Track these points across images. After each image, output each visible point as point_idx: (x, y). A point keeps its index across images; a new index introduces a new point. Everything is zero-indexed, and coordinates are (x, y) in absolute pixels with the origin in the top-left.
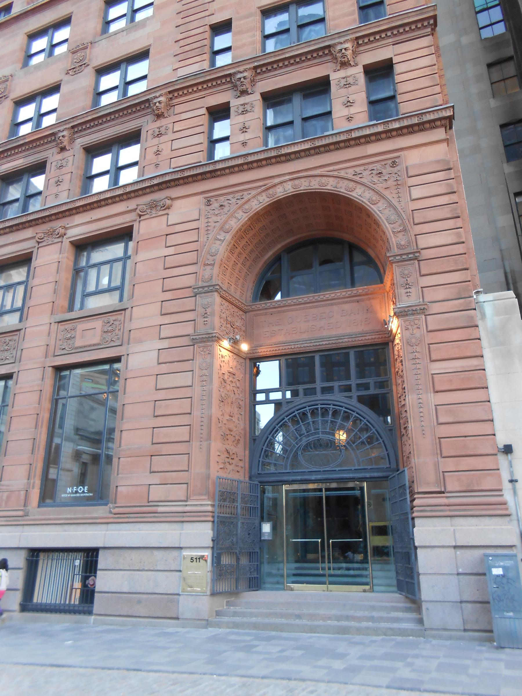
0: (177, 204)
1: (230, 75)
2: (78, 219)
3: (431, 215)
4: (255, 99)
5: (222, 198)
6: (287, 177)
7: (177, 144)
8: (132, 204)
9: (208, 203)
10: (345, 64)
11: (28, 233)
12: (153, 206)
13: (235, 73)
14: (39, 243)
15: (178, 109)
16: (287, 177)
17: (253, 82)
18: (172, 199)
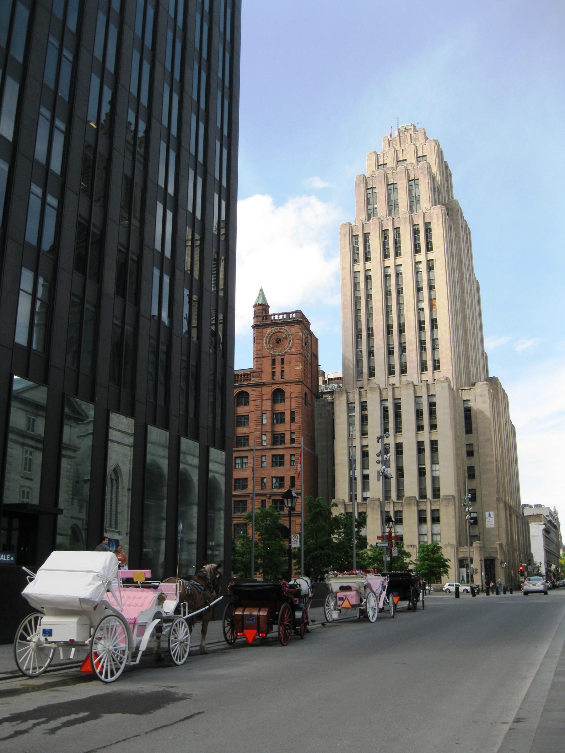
4: (271, 500)
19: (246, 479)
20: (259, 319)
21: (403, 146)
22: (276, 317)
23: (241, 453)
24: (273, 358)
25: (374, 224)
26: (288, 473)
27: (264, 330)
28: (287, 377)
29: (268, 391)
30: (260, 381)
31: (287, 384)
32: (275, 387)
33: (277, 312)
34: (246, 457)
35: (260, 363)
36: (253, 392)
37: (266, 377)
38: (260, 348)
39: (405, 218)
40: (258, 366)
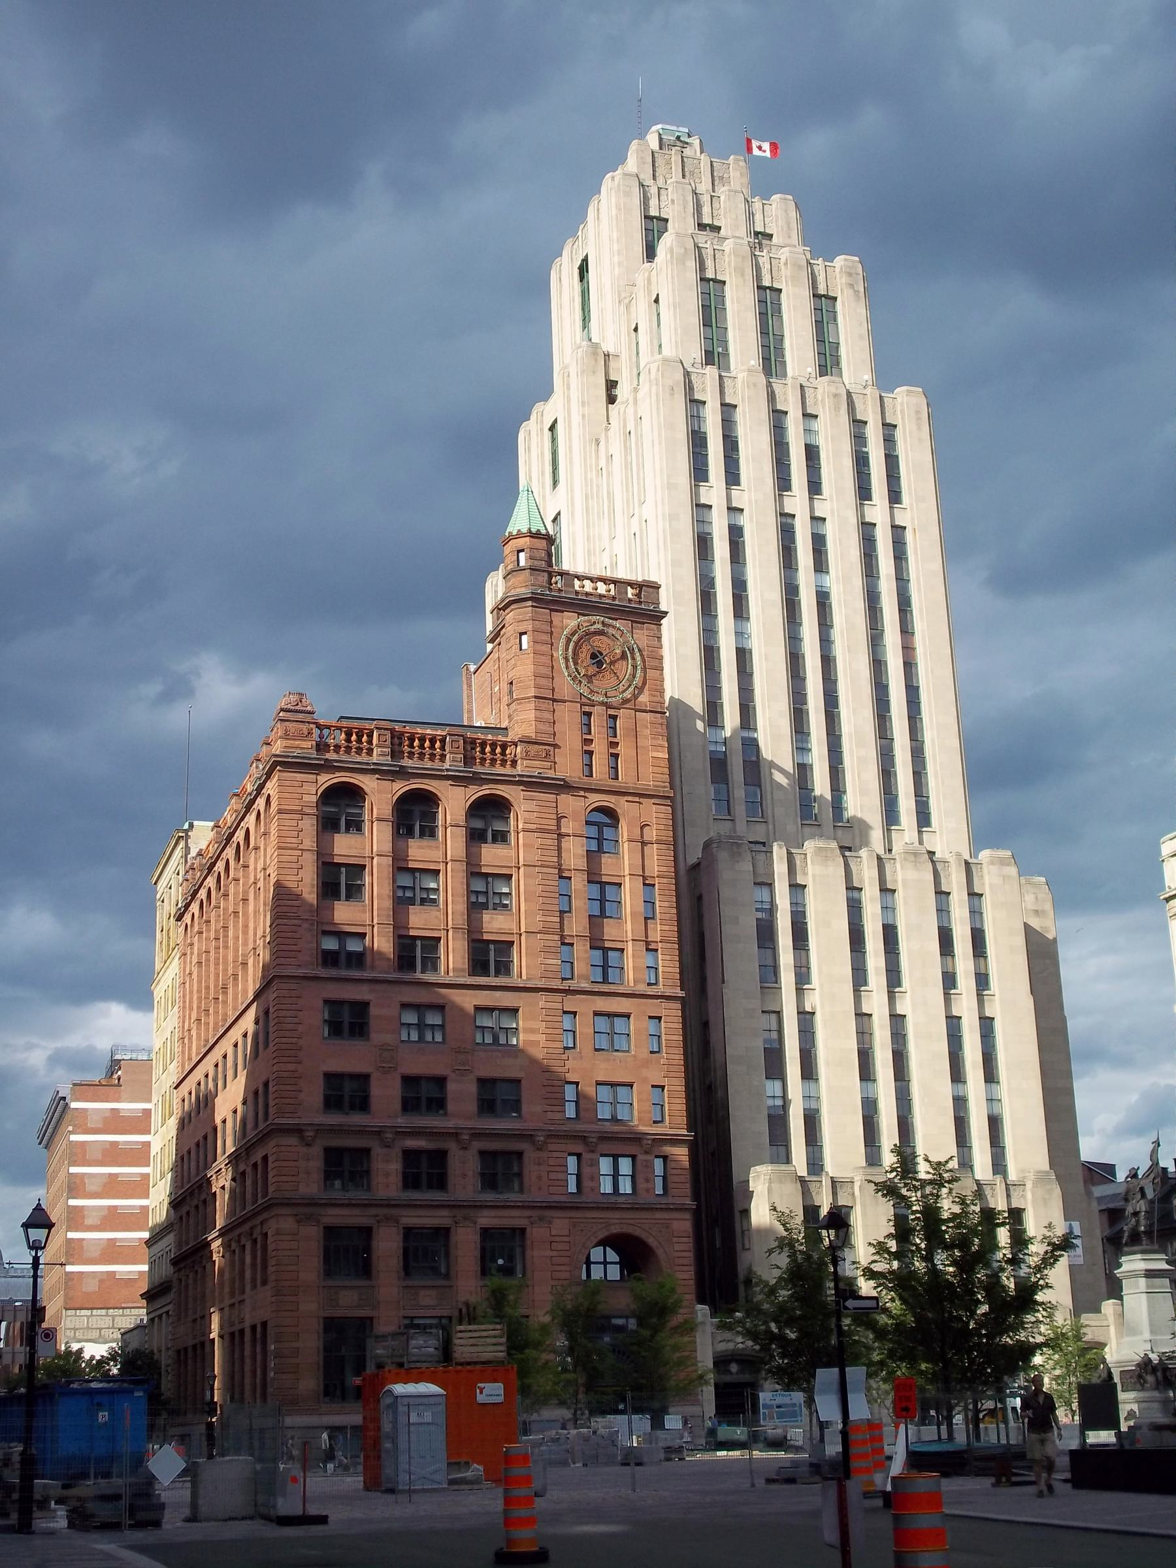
0: (556, 1221)
1: (585, 1137)
2: (486, 1212)
3: (681, 1261)
5: (582, 1224)
6: (616, 1221)
7: (552, 1176)
8: (528, 1213)
9: (574, 1226)
10: (646, 1153)
11: (445, 1212)
12: (541, 1219)
13: (588, 1137)
14: (456, 1223)
15: (551, 1147)
16: (616, 1221)
17: (597, 1144)
18: (552, 1217)
19: (518, 1081)
20: (540, 578)
21: (660, 182)
22: (588, 586)
23: (498, 994)
24: (587, 709)
25: (755, 385)
26: (645, 1072)
27: (556, 617)
28: (625, 776)
29: (575, 807)
30: (551, 774)
31: (630, 798)
32: (596, 799)
33: (596, 572)
34: (515, 1011)
35: (548, 716)
36: (532, 806)
37: (568, 766)
38: (546, 671)
39: (836, 396)
40: (542, 727)
